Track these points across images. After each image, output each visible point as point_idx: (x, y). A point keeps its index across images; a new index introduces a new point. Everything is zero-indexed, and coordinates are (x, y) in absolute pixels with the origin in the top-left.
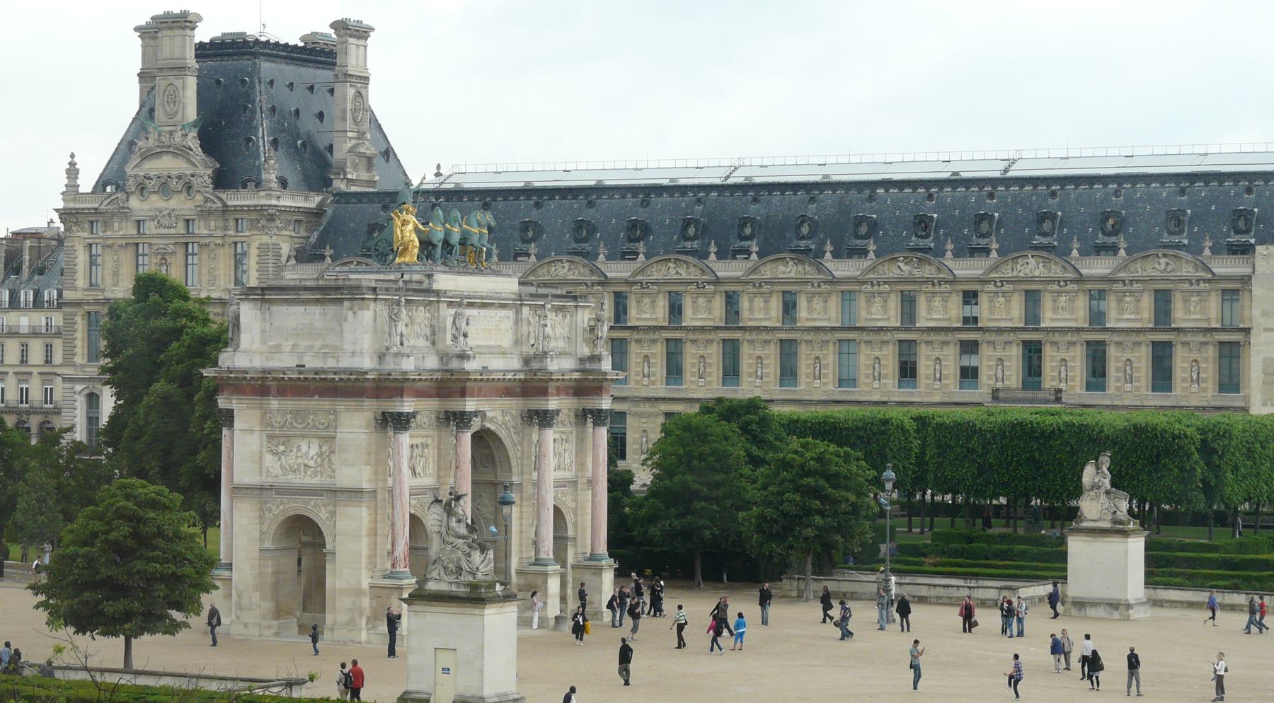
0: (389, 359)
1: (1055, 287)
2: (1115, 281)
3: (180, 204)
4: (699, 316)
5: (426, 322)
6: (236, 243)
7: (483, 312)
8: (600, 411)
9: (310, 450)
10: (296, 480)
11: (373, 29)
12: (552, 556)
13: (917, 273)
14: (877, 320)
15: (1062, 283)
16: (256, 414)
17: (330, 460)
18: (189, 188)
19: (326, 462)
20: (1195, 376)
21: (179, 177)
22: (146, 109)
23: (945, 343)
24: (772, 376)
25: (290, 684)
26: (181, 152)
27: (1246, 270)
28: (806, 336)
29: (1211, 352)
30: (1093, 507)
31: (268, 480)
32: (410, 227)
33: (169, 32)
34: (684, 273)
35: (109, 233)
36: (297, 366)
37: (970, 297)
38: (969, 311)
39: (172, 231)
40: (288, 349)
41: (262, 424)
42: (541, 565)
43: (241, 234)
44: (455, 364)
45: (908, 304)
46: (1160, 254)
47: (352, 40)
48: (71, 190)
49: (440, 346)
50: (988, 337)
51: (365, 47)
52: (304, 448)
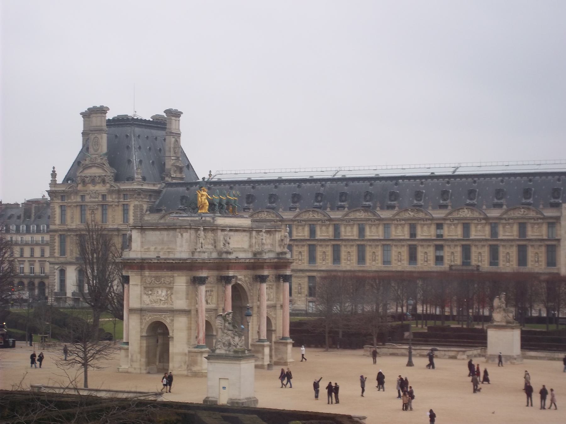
0: (196, 254)
1: (476, 222)
3: (100, 188)
4: (323, 235)
5: (212, 238)
6: (124, 205)
7: (236, 233)
8: (286, 275)
9: (162, 293)
10: (156, 306)
11: (182, 113)
12: (266, 338)
13: (417, 216)
14: (400, 236)
15: (479, 220)
17: (171, 297)
18: (104, 182)
19: (169, 299)
21: (99, 177)
22: (85, 148)
23: (429, 246)
26: (101, 166)
29: (543, 249)
31: (144, 306)
32: (204, 197)
34: (317, 216)
36: (157, 257)
37: (439, 226)
38: (439, 232)
39: (97, 200)
40: (153, 250)
41: (141, 282)
42: (262, 342)
43: (126, 201)
44: (224, 256)
45: (413, 228)
46: (521, 207)
47: (173, 118)
48: (53, 183)
49: (218, 248)
50: (447, 243)
51: (179, 121)
52: (160, 292)
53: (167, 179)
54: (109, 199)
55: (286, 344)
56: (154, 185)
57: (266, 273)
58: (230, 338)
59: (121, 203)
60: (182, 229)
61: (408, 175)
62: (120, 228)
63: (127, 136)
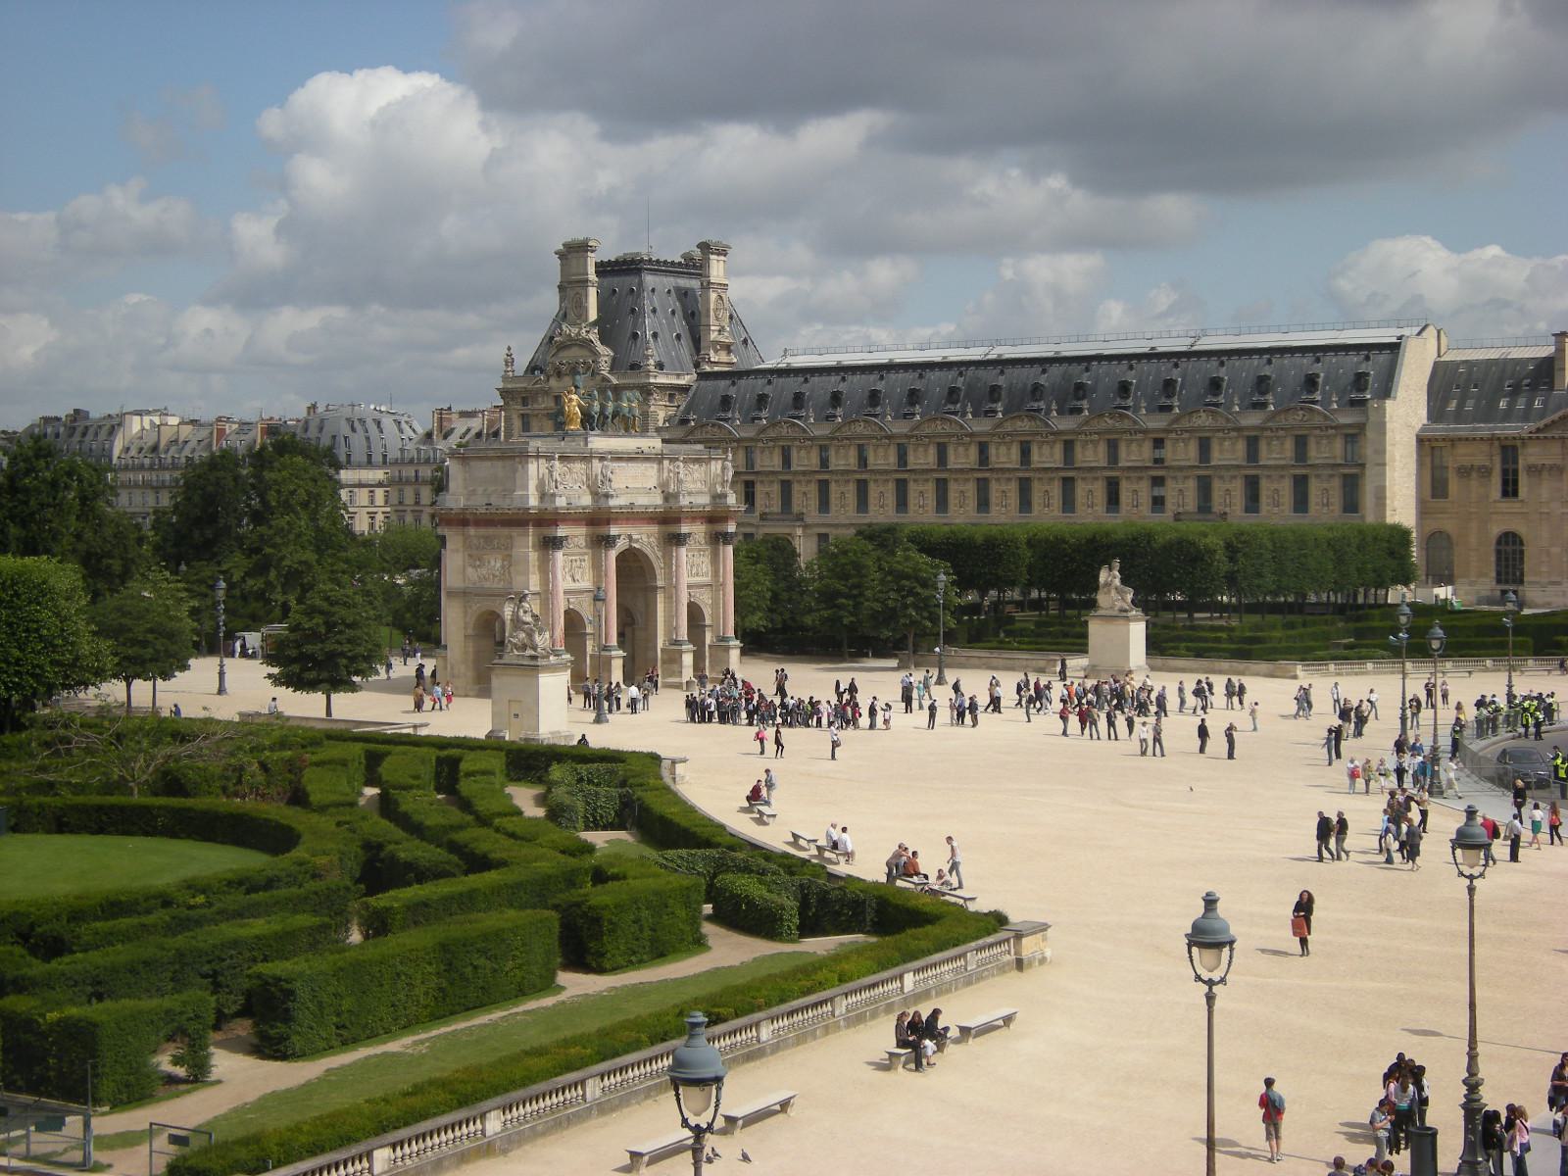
1: (1221, 434)
2: (1266, 429)
16: (460, 538)
20: (1325, 501)
23: (1141, 478)
24: (1013, 506)
25: (415, 727)
28: (1038, 475)
29: (1336, 483)
32: (574, 403)
33: (575, 255)
35: (535, 406)
37: (1159, 443)
45: (1113, 447)
50: (1172, 473)
52: (493, 563)
56: (678, 376)
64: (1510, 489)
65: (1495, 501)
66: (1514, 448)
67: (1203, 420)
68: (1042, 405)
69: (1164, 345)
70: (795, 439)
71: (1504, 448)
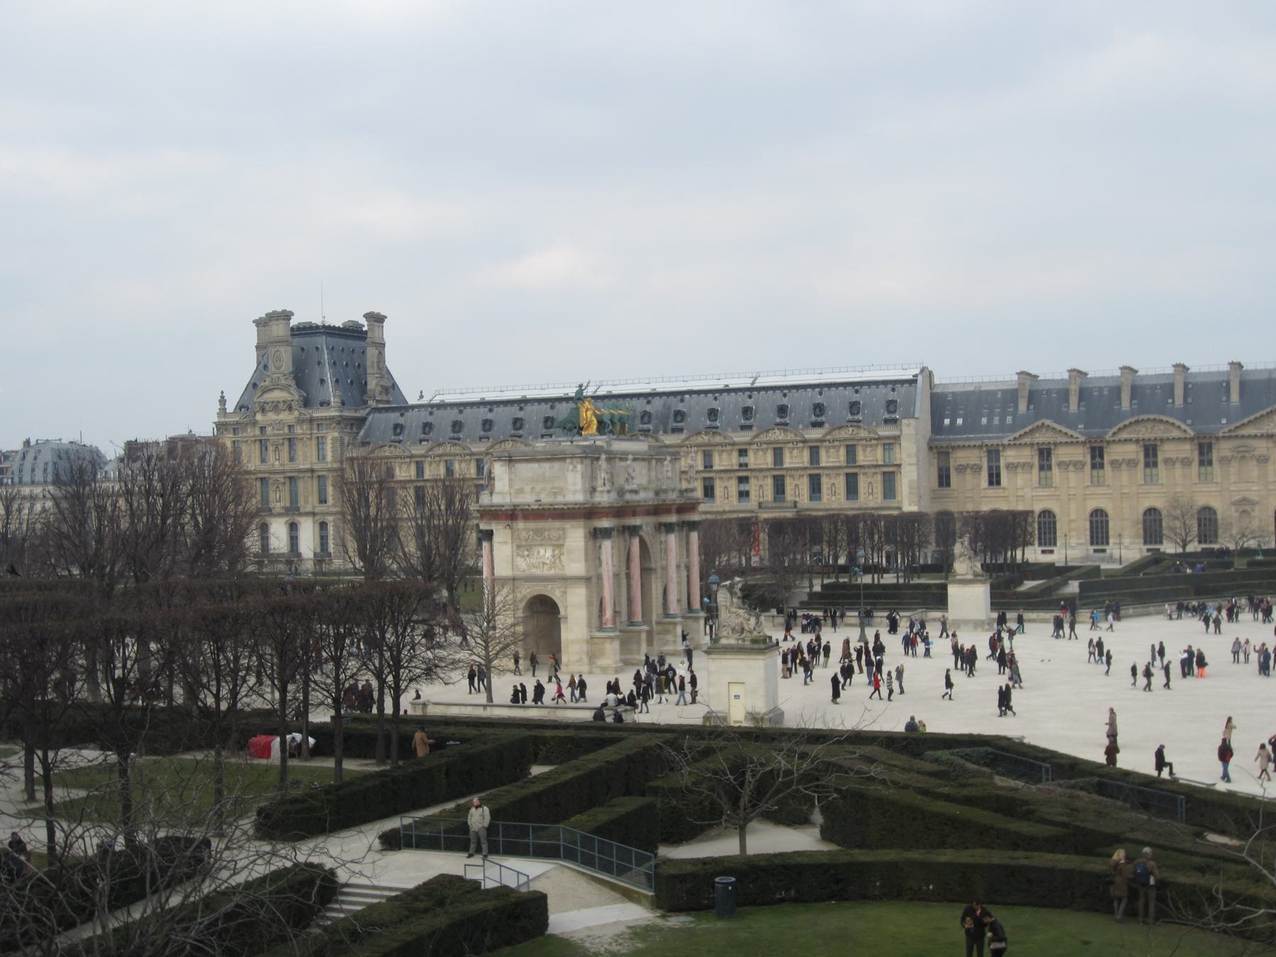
3: (285, 416)
6: (318, 438)
9: (546, 553)
11: (386, 317)
17: (560, 559)
18: (290, 408)
19: (557, 561)
21: (284, 402)
22: (261, 365)
23: (730, 478)
26: (285, 388)
27: (896, 433)
29: (879, 478)
30: (961, 567)
31: (518, 574)
35: (245, 434)
36: (536, 501)
37: (743, 453)
38: (743, 460)
39: (282, 432)
40: (529, 490)
44: (628, 497)
45: (708, 456)
47: (376, 324)
48: (223, 411)
50: (754, 474)
52: (542, 552)
53: (370, 402)
54: (298, 430)
55: (697, 619)
57: (637, 521)
58: (741, 619)
59: (314, 436)
60: (574, 460)
61: (695, 388)
62: (315, 467)
63: (317, 348)
64: (994, 479)
65: (984, 489)
66: (997, 452)
67: (777, 435)
68: (650, 427)
69: (735, 383)
70: (456, 455)
71: (989, 452)
